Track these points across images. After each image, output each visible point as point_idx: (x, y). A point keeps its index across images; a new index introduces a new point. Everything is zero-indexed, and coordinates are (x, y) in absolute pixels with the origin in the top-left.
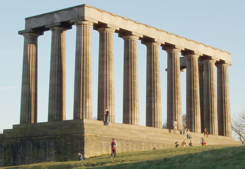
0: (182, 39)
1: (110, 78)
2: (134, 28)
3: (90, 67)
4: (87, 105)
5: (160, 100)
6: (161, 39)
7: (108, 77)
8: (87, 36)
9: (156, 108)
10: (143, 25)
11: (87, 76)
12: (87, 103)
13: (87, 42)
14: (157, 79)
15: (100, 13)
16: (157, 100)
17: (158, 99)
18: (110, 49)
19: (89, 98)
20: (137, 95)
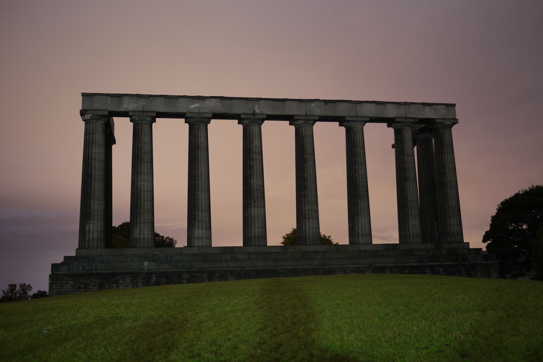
0: (313, 105)
1: (139, 186)
2: (192, 106)
3: (93, 176)
4: (87, 229)
5: (256, 203)
6: (258, 111)
7: (136, 184)
8: (91, 136)
9: (250, 216)
10: (213, 100)
11: (89, 189)
12: (87, 226)
13: (91, 142)
14: (252, 172)
15: (116, 99)
16: (250, 204)
17: (253, 203)
18: (140, 145)
19: (90, 220)
20: (200, 202)
